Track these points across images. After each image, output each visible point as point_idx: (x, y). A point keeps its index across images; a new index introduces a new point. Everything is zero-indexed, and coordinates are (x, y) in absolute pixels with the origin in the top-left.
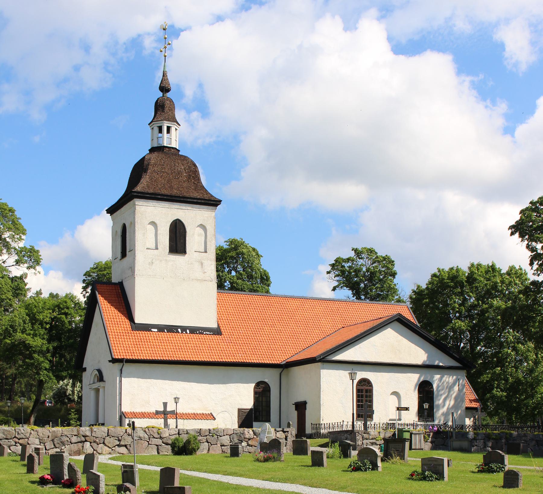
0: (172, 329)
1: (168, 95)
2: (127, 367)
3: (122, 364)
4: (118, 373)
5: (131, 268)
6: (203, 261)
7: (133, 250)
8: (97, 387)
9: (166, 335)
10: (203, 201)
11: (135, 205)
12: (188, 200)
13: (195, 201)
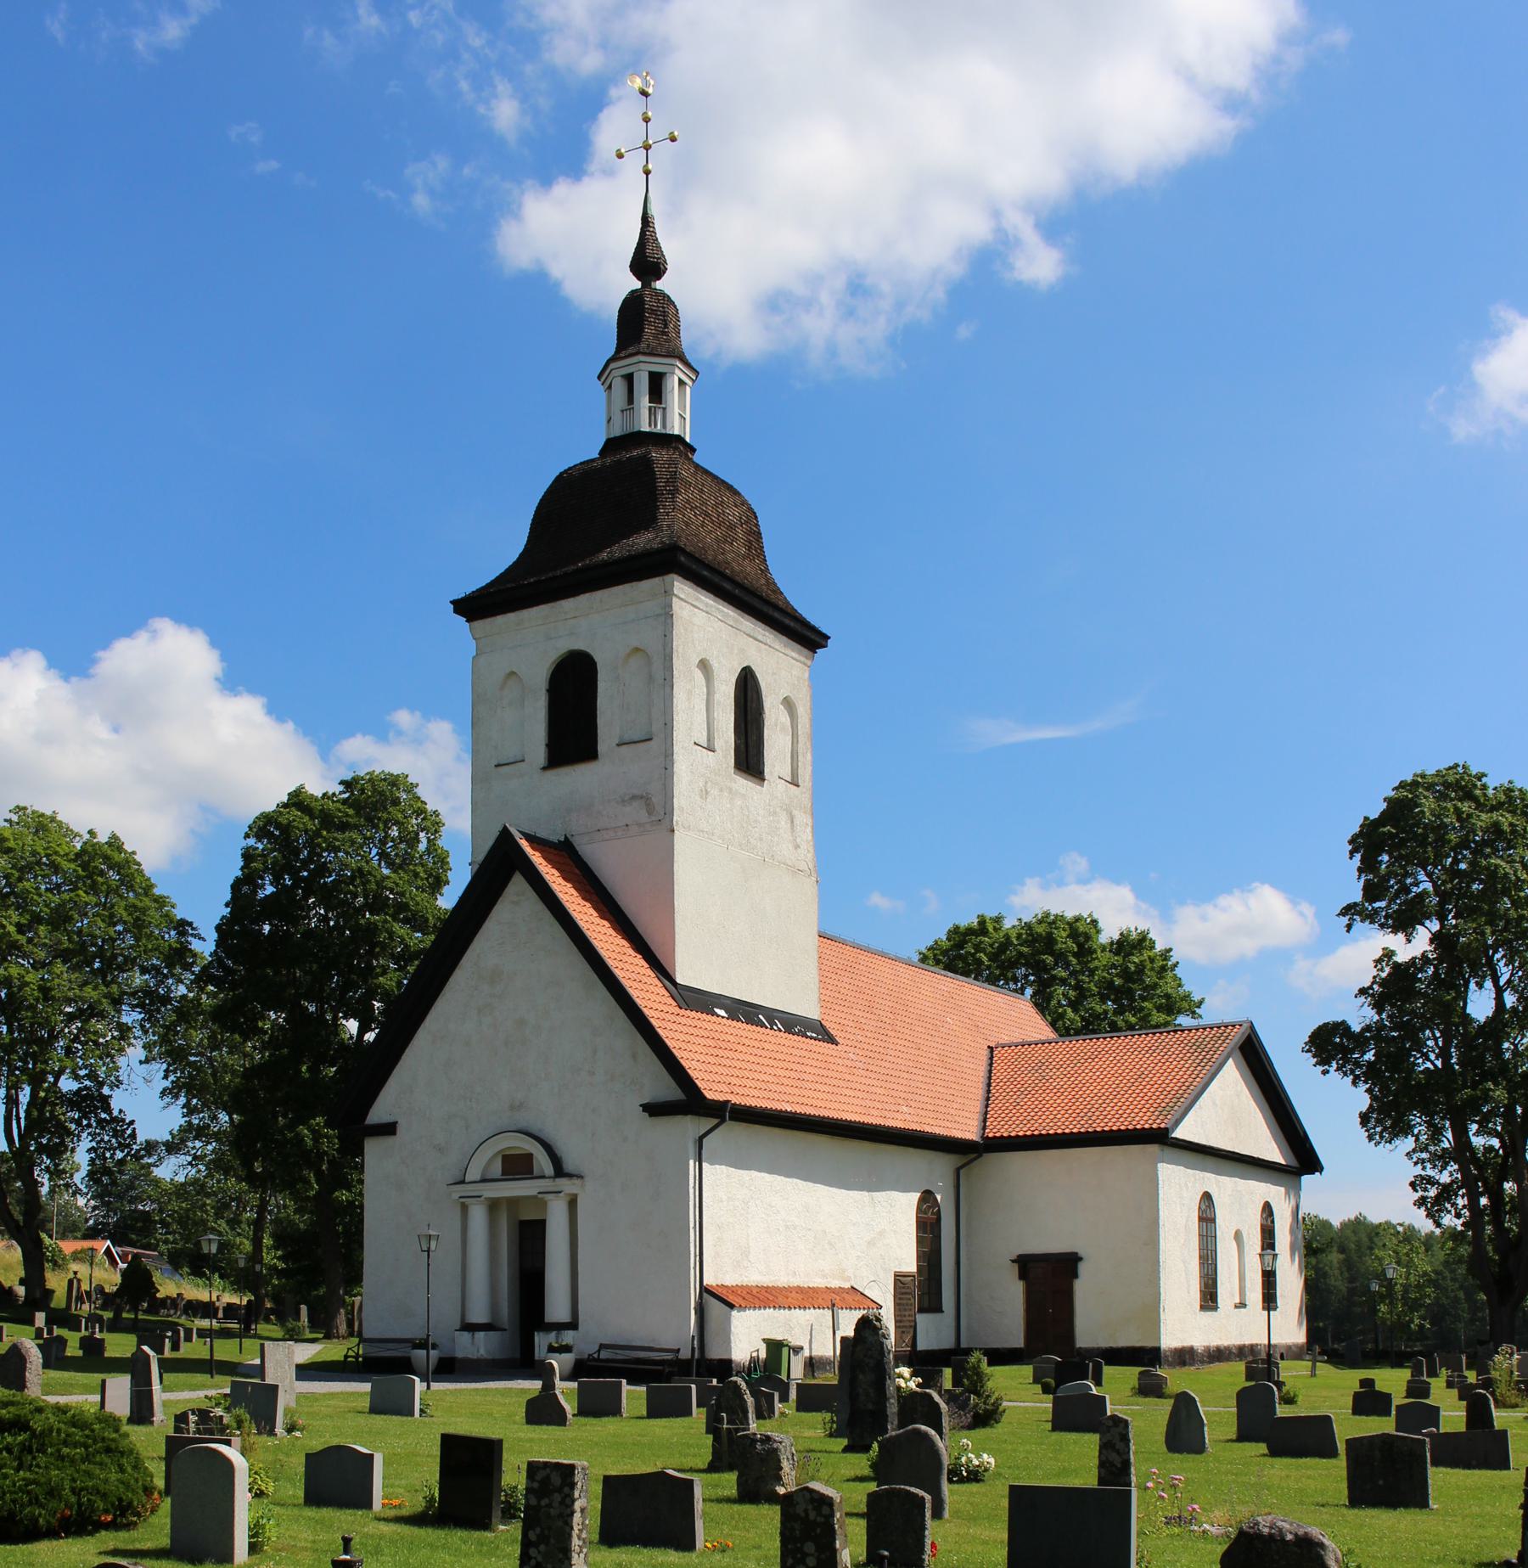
1: (658, 285)
2: (731, 1132)
3: (716, 1121)
4: (692, 1149)
5: (645, 799)
6: (796, 812)
7: (655, 737)
8: (533, 1192)
10: (798, 627)
11: (668, 593)
12: (776, 615)
13: (787, 621)
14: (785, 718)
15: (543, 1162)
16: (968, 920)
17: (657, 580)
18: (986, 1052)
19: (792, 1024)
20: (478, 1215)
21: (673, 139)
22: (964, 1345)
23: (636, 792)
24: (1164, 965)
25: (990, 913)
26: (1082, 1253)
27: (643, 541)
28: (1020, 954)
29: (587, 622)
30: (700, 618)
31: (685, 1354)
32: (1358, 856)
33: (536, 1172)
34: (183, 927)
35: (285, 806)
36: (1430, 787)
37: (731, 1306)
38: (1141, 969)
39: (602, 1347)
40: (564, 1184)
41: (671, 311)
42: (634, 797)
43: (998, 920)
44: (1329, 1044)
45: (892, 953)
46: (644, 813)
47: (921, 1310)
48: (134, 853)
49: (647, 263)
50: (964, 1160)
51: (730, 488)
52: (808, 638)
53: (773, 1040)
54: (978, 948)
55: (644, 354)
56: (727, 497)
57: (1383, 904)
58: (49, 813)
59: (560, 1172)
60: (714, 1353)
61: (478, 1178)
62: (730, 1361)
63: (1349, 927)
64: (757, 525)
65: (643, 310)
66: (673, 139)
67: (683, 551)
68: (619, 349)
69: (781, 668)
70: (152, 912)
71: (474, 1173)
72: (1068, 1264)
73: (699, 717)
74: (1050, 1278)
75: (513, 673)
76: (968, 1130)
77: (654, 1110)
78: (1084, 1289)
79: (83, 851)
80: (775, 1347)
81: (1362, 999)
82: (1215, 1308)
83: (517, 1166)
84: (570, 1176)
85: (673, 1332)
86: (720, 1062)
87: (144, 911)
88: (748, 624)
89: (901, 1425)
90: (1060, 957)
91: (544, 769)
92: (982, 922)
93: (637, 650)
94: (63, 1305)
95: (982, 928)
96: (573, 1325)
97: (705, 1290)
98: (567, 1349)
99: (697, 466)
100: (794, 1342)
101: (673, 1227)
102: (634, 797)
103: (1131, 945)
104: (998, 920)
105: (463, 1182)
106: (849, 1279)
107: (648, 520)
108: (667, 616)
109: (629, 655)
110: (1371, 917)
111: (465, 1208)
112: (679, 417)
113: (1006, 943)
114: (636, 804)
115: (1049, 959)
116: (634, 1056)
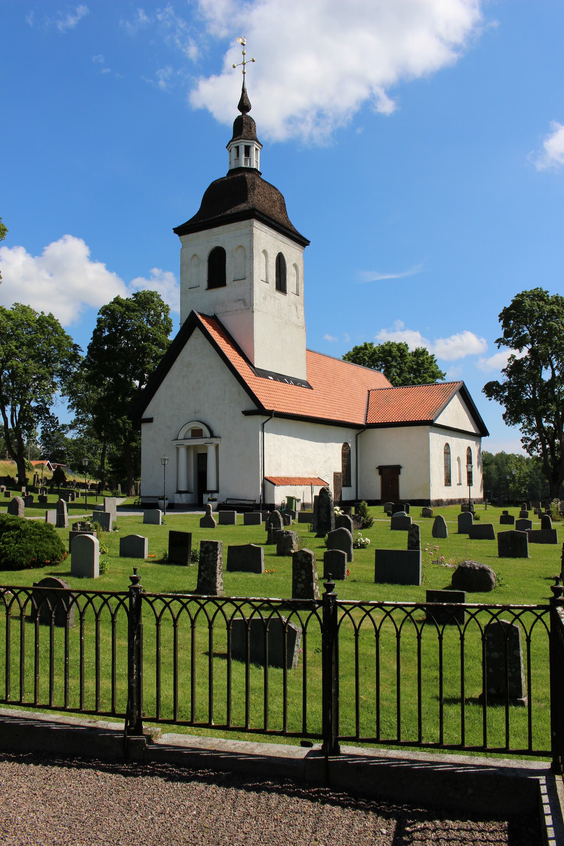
0: (279, 378)
1: (248, 114)
2: (275, 422)
3: (269, 417)
5: (243, 301)
6: (298, 305)
7: (247, 278)
8: (203, 443)
9: (278, 384)
10: (299, 238)
11: (252, 225)
12: (291, 234)
13: (295, 236)
14: (294, 271)
15: (206, 432)
16: (361, 344)
17: (247, 221)
18: (367, 392)
19: (297, 382)
20: (183, 451)
21: (253, 61)
22: (359, 499)
23: (240, 298)
24: (432, 361)
25: (368, 342)
26: (402, 465)
27: (242, 207)
28: (379, 357)
29: (222, 236)
30: (263, 235)
31: (258, 502)
32: (502, 321)
33: (204, 436)
34: (75, 347)
35: (113, 303)
36: (528, 296)
37: (275, 485)
38: (423, 362)
39: (228, 499)
40: (213, 440)
41: (253, 123)
42: (239, 300)
43: (371, 344)
44: (492, 389)
45: (333, 357)
46: (243, 305)
47: (343, 486)
48: (58, 320)
49: (244, 106)
50: (359, 431)
51: (274, 187)
52: (302, 242)
53: (290, 388)
54: (364, 354)
55: (243, 139)
56: (273, 191)
57: (511, 339)
58: (27, 305)
59: (212, 436)
60: (268, 502)
61: (183, 438)
62: (274, 505)
63: (499, 347)
64: (284, 201)
65: (243, 123)
66: (253, 61)
67: (257, 210)
68: (233, 137)
69: (293, 253)
70: (64, 342)
71: (181, 436)
72: (396, 470)
73: (263, 271)
74: (390, 474)
75: (195, 255)
76: (361, 421)
77: (247, 413)
78: (402, 478)
79: (39, 319)
80: (290, 499)
81: (504, 373)
82: (450, 485)
83: (197, 434)
84: (216, 437)
85: (253, 494)
86: (271, 396)
87: (61, 341)
88: (281, 237)
89: (336, 528)
90: (394, 358)
91: (207, 289)
92: (366, 345)
93: (240, 246)
94: (32, 484)
95: (365, 347)
96: (217, 491)
97: (265, 479)
98: (215, 500)
99: (262, 180)
100: (297, 498)
101: (253, 456)
102: (239, 300)
103: (420, 353)
104: (371, 344)
105: (177, 439)
106: (317, 475)
107: (244, 199)
108: (251, 234)
109: (237, 248)
110: (507, 343)
111: (178, 449)
112: (256, 162)
113: (374, 353)
114: (240, 302)
115: (390, 359)
116: (239, 394)
